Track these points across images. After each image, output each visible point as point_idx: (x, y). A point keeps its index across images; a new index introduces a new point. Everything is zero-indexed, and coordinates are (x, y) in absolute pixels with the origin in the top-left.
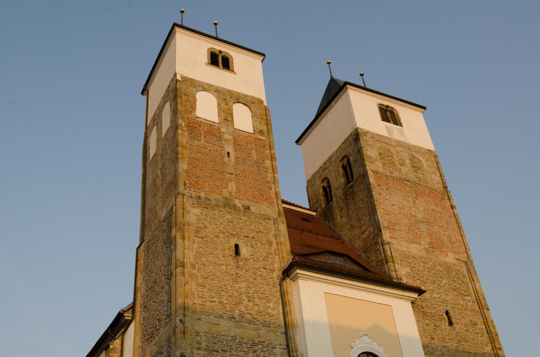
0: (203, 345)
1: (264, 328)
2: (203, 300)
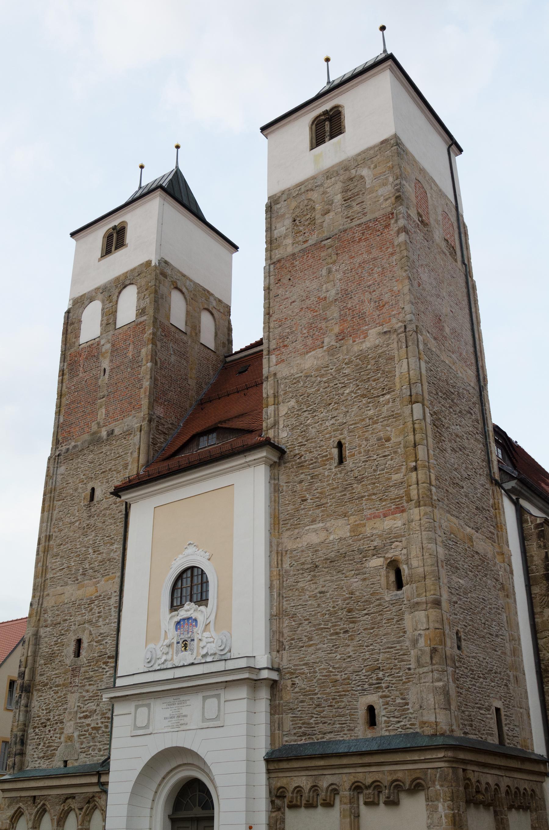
0: (49, 622)
1: (103, 579)
2: (54, 571)
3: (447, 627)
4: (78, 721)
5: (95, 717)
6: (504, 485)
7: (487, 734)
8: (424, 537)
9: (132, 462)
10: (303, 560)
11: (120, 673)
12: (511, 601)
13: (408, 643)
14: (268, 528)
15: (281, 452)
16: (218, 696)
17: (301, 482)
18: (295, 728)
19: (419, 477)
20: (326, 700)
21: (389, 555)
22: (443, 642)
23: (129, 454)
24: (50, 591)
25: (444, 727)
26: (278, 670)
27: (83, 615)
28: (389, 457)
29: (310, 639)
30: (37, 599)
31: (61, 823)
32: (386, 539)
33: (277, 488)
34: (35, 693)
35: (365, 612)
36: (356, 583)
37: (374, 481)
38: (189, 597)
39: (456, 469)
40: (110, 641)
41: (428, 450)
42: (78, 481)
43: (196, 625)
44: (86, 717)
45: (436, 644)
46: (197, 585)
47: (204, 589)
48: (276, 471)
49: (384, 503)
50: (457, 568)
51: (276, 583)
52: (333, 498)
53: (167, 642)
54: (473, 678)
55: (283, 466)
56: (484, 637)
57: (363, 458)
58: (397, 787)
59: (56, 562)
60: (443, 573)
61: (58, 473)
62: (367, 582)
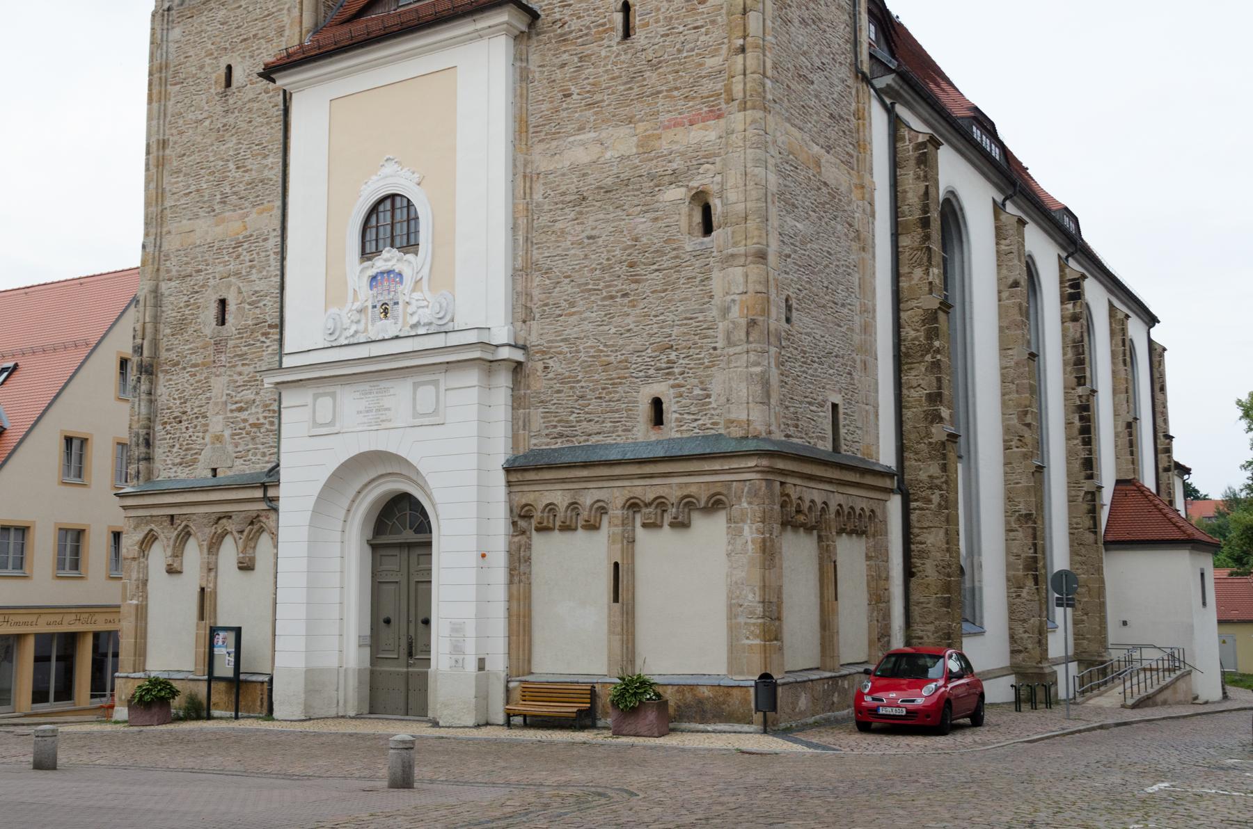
0: (174, 273)
1: (255, 210)
2: (176, 196)
3: (773, 291)
4: (229, 415)
5: (254, 410)
6: (875, 82)
7: (818, 437)
8: (750, 157)
9: (291, 25)
10: (563, 188)
11: (287, 350)
12: (867, 256)
13: (715, 313)
14: (511, 138)
15: (534, 16)
16: (436, 383)
17: (563, 65)
18: (547, 427)
19: (748, 63)
20: (593, 390)
21: (694, 184)
22: (766, 312)
23: (285, 12)
24: (172, 226)
25: (759, 427)
26: (524, 348)
27: (226, 263)
28: (703, 30)
29: (572, 305)
30: (152, 238)
31: (214, 550)
32: (691, 159)
33: (524, 74)
34: (161, 375)
35: (655, 267)
36: (642, 224)
37: (677, 67)
38: (389, 241)
39: (804, 54)
40: (270, 304)
41: (764, 20)
42: (203, 54)
43: (401, 282)
44: (240, 410)
45: (756, 314)
46: (401, 222)
47: (412, 230)
48: (524, 47)
49: (691, 104)
50: (793, 205)
51: (522, 222)
52: (613, 93)
53: (357, 305)
54: (805, 363)
55: (535, 38)
56: (824, 306)
57: (662, 31)
58: (689, 504)
59: (177, 183)
60: (773, 211)
61: (170, 38)
62: (660, 224)
